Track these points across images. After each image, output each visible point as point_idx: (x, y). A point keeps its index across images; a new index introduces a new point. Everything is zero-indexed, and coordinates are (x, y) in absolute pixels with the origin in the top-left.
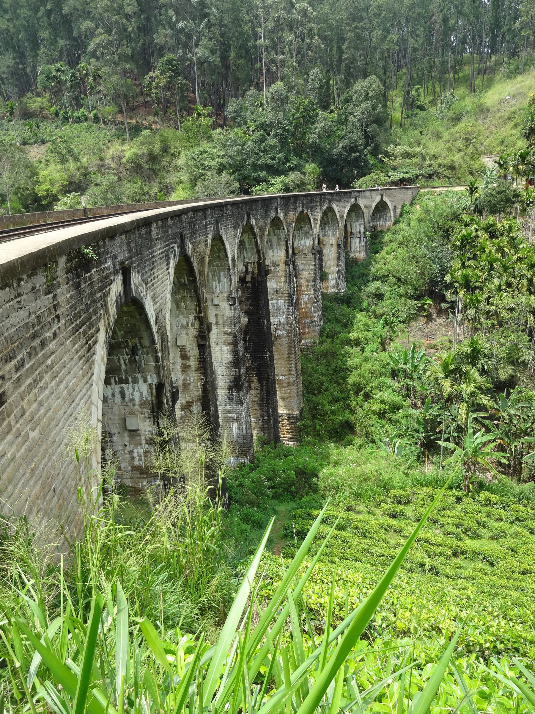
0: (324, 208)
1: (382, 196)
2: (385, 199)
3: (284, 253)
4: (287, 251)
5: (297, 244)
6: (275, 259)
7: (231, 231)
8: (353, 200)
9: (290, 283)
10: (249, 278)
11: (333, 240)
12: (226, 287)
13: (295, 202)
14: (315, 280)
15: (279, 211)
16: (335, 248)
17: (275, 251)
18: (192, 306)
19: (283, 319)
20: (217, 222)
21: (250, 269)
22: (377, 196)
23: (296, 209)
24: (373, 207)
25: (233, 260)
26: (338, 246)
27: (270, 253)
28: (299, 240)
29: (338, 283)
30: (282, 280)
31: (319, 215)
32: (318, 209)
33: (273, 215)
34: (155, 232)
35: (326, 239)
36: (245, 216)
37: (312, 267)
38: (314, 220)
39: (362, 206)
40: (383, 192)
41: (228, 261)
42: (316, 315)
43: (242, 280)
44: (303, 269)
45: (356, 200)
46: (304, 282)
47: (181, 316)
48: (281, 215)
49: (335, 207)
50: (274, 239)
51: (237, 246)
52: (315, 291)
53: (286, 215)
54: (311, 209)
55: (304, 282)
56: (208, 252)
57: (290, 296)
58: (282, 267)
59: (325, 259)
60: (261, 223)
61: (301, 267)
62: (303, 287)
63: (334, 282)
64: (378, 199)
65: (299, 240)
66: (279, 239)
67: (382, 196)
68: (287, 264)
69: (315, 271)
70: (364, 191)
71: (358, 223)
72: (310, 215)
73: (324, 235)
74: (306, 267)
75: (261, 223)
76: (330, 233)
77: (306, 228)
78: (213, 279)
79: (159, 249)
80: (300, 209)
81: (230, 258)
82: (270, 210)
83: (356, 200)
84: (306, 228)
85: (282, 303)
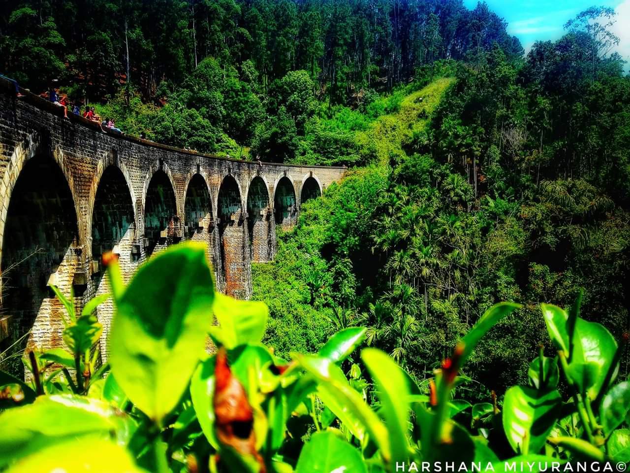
0: (253, 177)
1: (311, 173)
2: (313, 176)
7: (137, 173)
8: (282, 173)
9: (214, 247)
13: (220, 165)
14: (243, 247)
15: (201, 169)
17: (199, 213)
20: (114, 152)
22: (305, 173)
23: (221, 171)
24: (303, 183)
28: (227, 207)
29: (269, 254)
31: (247, 183)
32: (246, 177)
33: (194, 171)
36: (158, 162)
40: (312, 169)
41: (131, 202)
44: (232, 236)
45: (285, 174)
47: (53, 249)
48: (204, 174)
53: (210, 175)
60: (178, 175)
64: (307, 176)
65: (227, 207)
67: (311, 173)
71: (288, 198)
72: (238, 182)
75: (178, 175)
78: (114, 224)
80: (226, 173)
81: (134, 200)
83: (285, 174)
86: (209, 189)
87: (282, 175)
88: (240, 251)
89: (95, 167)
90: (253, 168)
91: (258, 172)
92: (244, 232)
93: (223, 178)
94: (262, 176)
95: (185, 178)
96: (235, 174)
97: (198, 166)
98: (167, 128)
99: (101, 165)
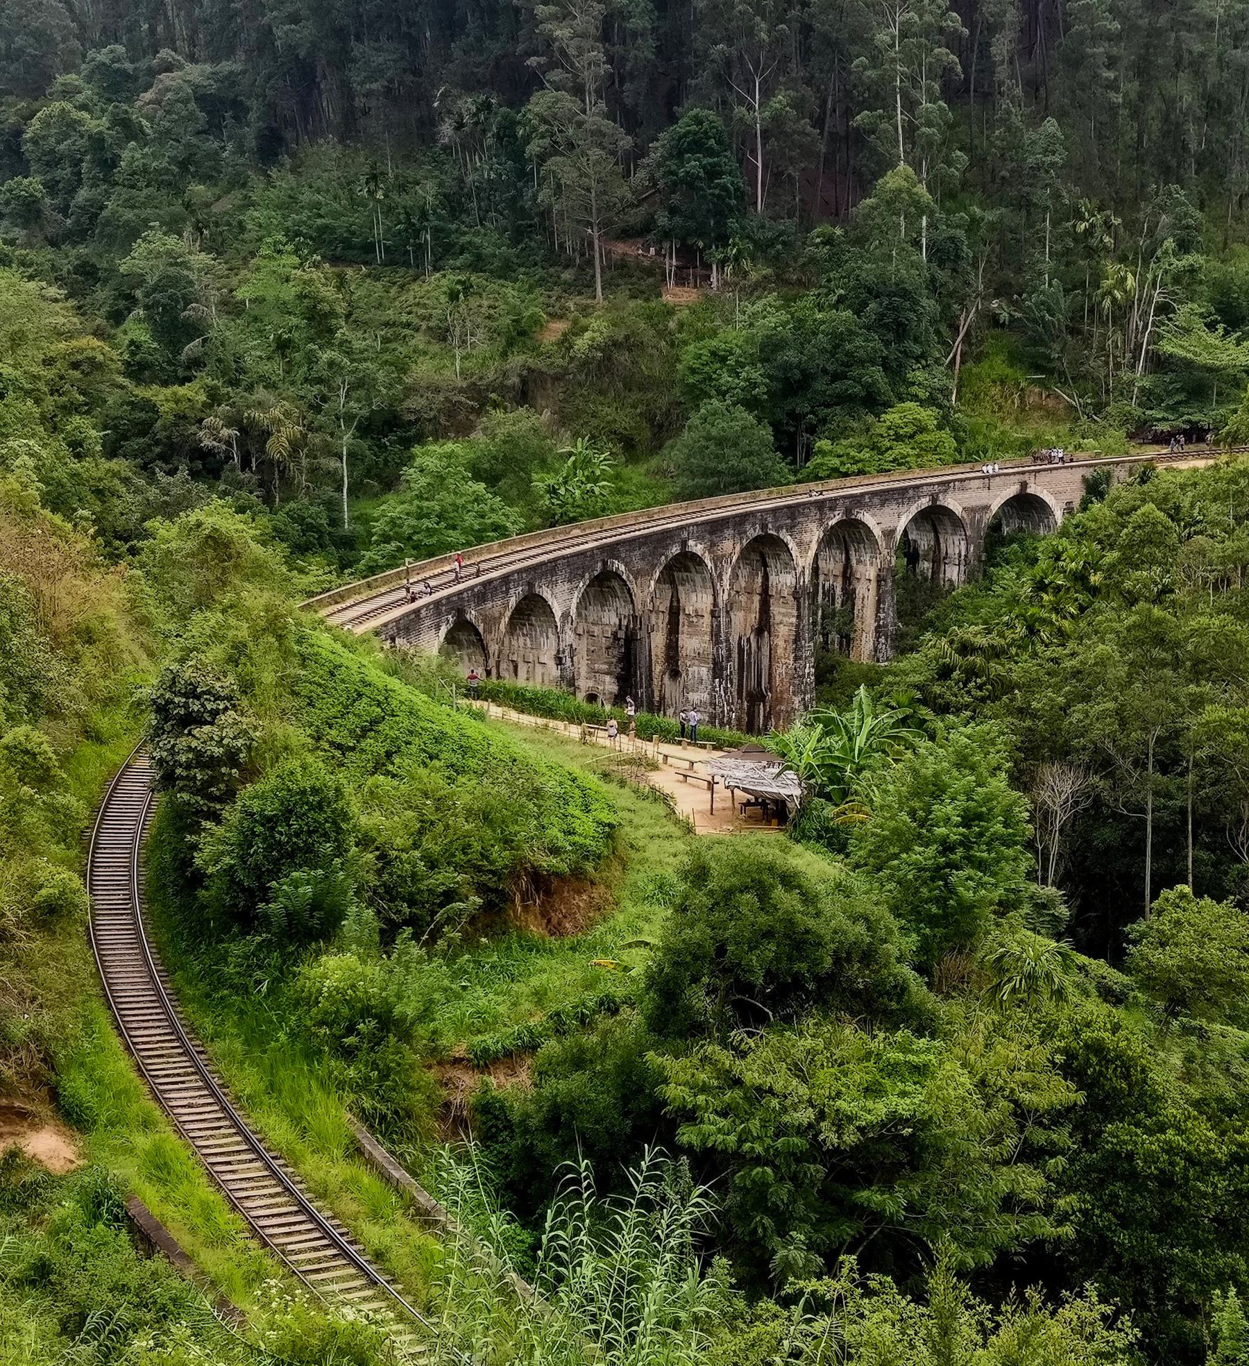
0: (832, 522)
3: (711, 598)
4: (715, 596)
5: (773, 579)
6: (699, 606)
7: (563, 587)
10: (621, 634)
11: (872, 573)
12: (555, 644)
15: (691, 543)
16: (873, 586)
18: (481, 659)
19: (705, 697)
21: (625, 623)
23: (742, 533)
25: (566, 615)
26: (880, 580)
27: (693, 596)
29: (876, 649)
30: (707, 638)
32: (813, 526)
33: (675, 550)
34: (423, 612)
35: (861, 568)
37: (794, 620)
38: (799, 544)
39: (957, 509)
40: (1026, 477)
42: (797, 700)
43: (615, 634)
45: (934, 498)
46: (781, 643)
48: (696, 547)
49: (868, 518)
50: (698, 578)
51: (575, 601)
52: (796, 659)
53: (712, 546)
54: (791, 529)
55: (781, 643)
56: (508, 614)
57: (715, 663)
58: (707, 619)
59: (858, 602)
60: (639, 565)
61: (778, 618)
62: (780, 651)
63: (870, 646)
64: (1012, 490)
66: (704, 579)
67: (1024, 485)
68: (713, 613)
69: (798, 626)
70: (961, 480)
71: (956, 538)
73: (859, 562)
74: (785, 619)
76: (867, 558)
77: (784, 556)
79: (428, 622)
80: (753, 532)
81: (558, 614)
82: (666, 547)
83: (934, 498)
84: (784, 556)
85: (704, 671)
86: (710, 565)
87: (925, 502)
88: (791, 646)
89: (506, 606)
90: (832, 509)
91: (848, 511)
92: (799, 617)
93: (745, 542)
94: (860, 516)
95: (654, 567)
96: (778, 529)
97: (684, 543)
98: (786, 367)
99: (513, 602)
